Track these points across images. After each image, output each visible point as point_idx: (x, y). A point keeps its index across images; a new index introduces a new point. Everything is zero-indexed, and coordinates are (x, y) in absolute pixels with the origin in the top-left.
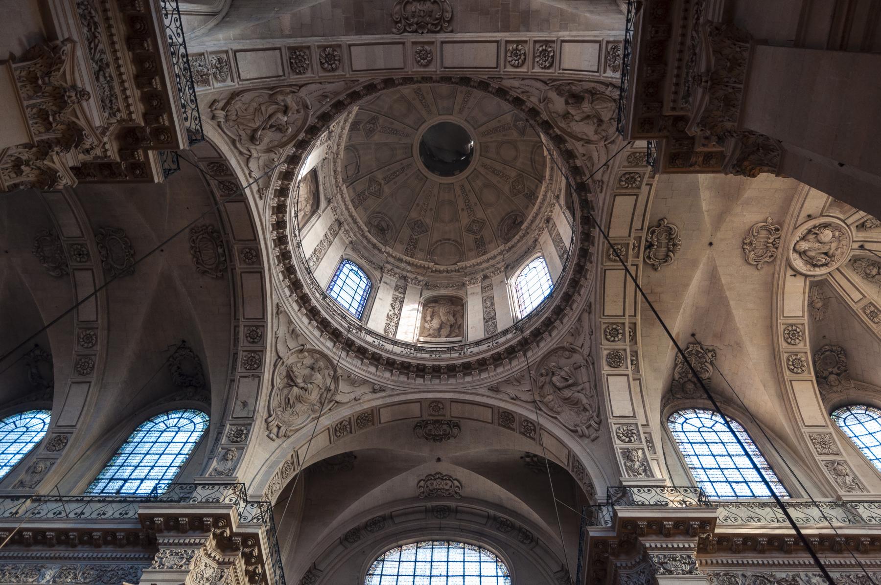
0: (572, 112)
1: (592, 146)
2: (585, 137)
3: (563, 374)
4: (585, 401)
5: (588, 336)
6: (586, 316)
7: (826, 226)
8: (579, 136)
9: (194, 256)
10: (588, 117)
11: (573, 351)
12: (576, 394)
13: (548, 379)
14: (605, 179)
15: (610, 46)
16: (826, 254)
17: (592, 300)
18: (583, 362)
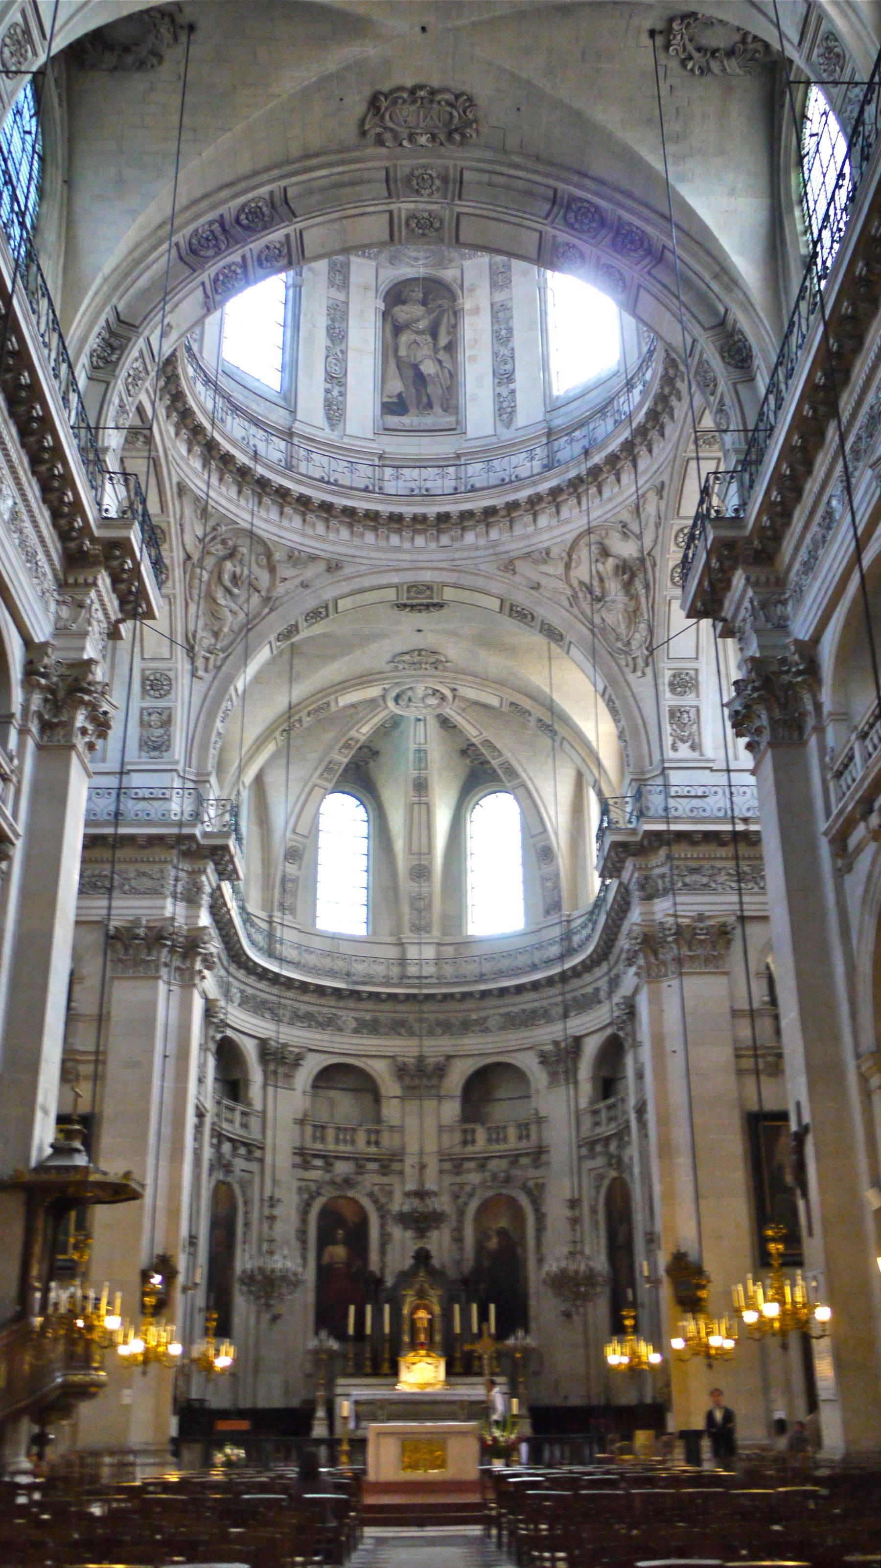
0: (611, 561)
1: (560, 570)
2: (573, 564)
3: (238, 570)
4: (226, 630)
5: (297, 581)
6: (321, 566)
7: (443, 698)
8: (574, 557)
9: (413, 91)
10: (601, 580)
11: (272, 570)
12: (228, 614)
13: (221, 553)
14: (517, 579)
15: (692, 673)
16: (410, 700)
17: (348, 571)
18: (263, 593)
